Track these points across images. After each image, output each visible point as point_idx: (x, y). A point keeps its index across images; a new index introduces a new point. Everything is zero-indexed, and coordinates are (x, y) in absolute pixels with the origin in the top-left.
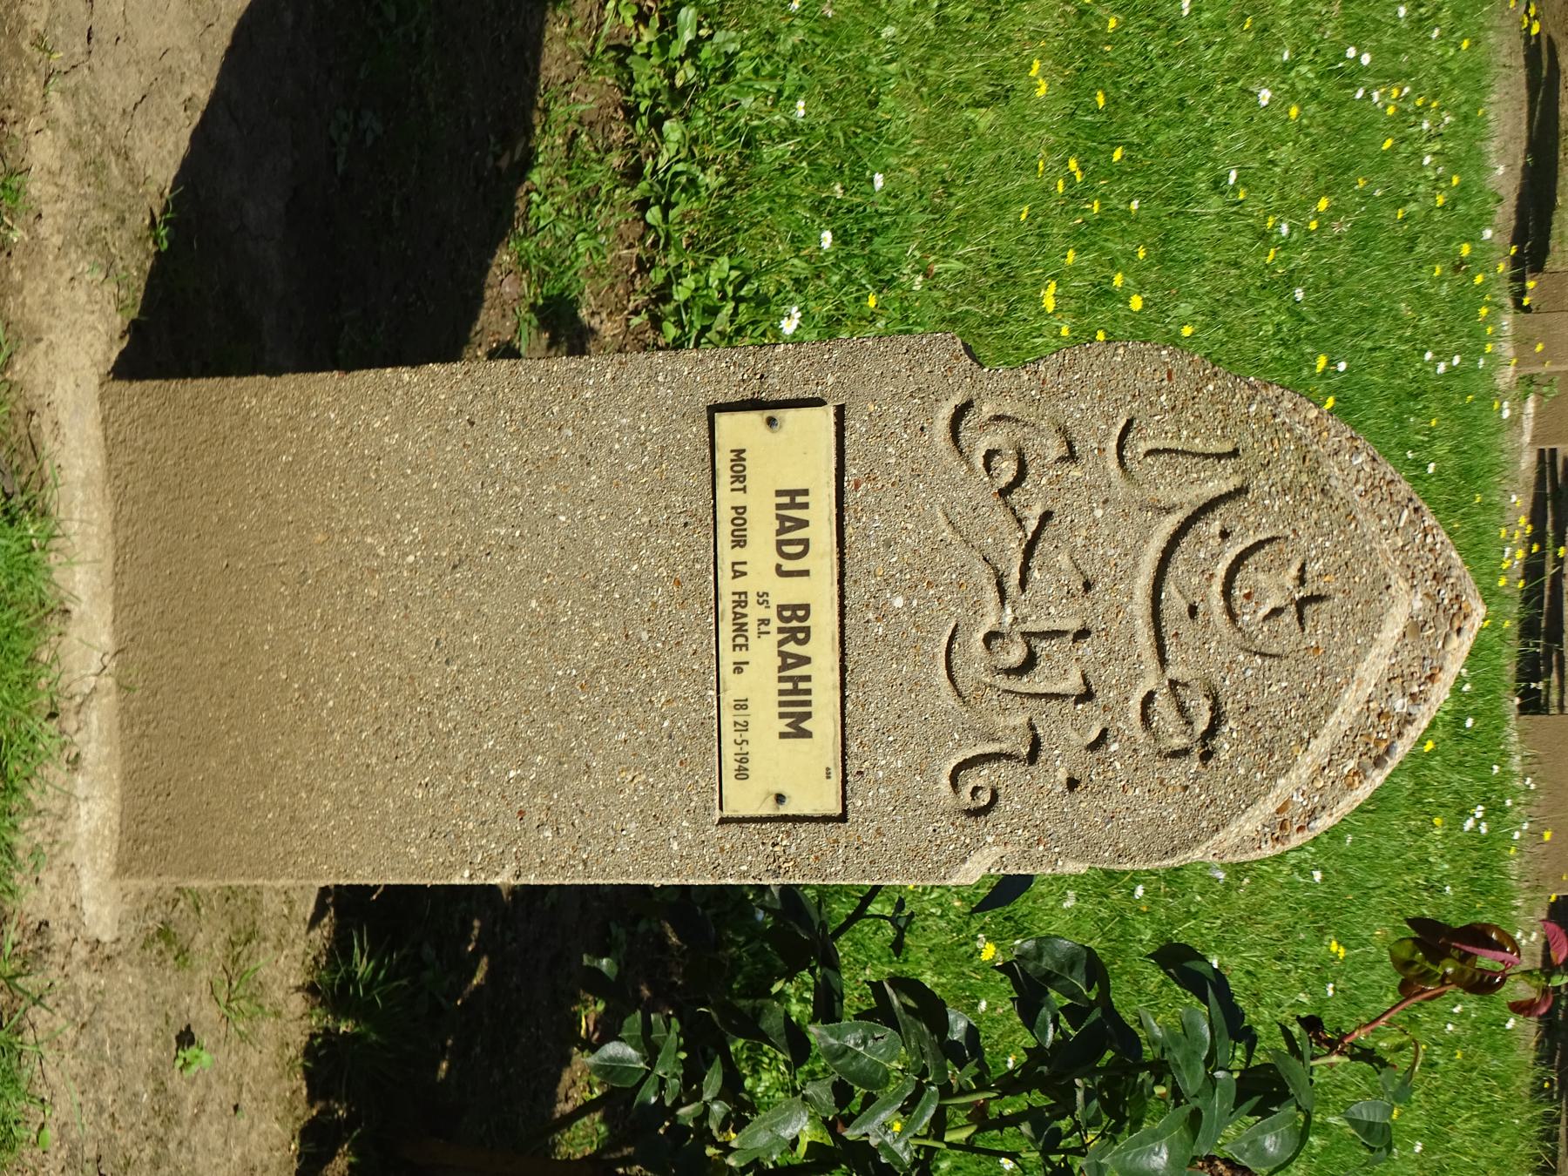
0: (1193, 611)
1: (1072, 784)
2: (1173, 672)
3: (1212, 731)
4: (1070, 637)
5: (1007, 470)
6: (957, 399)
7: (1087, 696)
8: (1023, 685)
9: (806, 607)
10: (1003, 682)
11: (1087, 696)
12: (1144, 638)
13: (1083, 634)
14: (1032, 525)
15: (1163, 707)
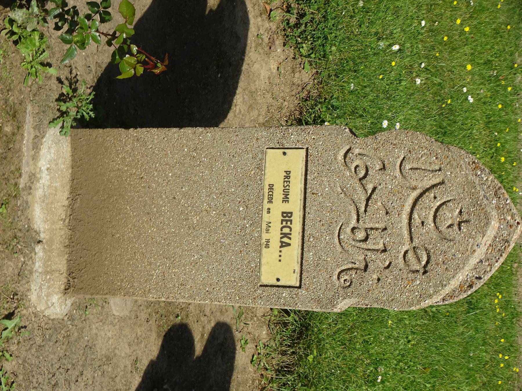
0: (423, 223)
1: (379, 280)
2: (414, 244)
3: (425, 266)
4: (380, 231)
5: (362, 173)
6: (348, 147)
7: (385, 251)
8: (363, 245)
9: (291, 213)
10: (358, 244)
11: (385, 251)
12: (406, 233)
13: (385, 229)
14: (369, 192)
15: (410, 255)
